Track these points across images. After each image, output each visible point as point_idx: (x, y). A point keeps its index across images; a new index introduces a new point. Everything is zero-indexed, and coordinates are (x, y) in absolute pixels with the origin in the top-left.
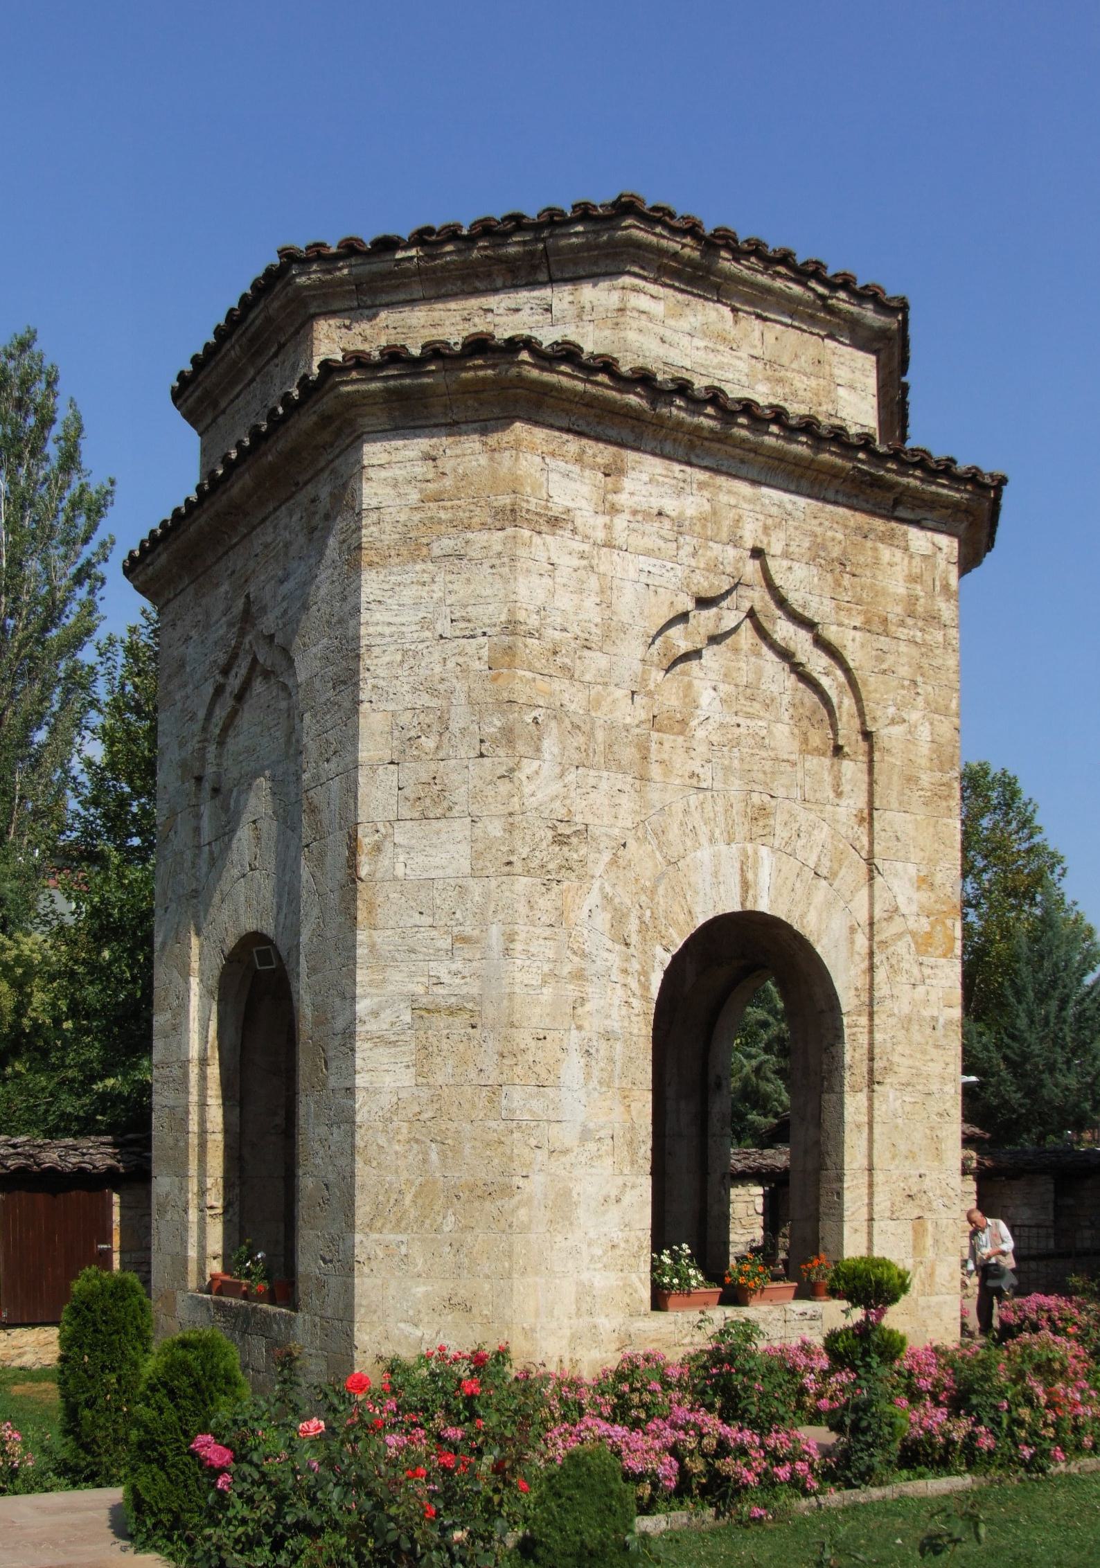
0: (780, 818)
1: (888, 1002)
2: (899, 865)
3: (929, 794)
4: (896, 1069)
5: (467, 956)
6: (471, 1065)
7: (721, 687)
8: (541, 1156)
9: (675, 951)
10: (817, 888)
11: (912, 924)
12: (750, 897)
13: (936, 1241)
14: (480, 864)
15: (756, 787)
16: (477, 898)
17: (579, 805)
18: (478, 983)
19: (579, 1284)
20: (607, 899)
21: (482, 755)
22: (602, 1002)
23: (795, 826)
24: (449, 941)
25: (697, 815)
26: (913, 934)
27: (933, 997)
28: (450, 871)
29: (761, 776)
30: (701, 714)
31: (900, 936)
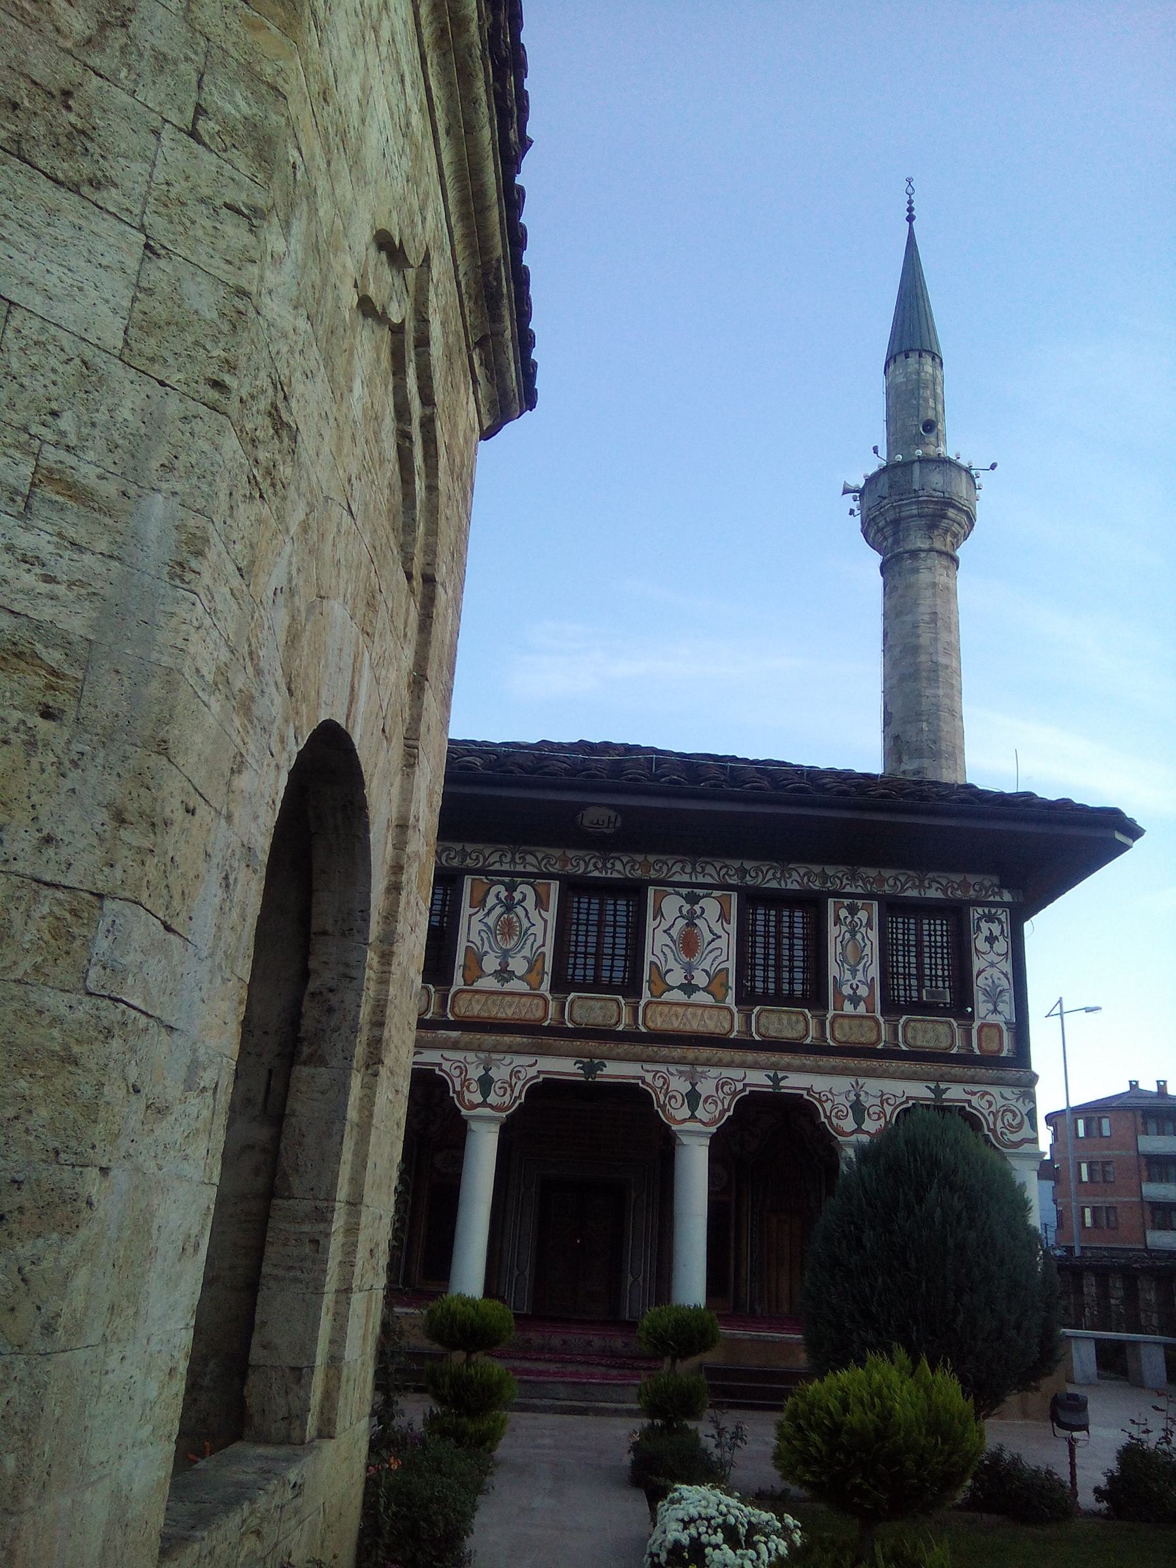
5: (71, 533)
6: (22, 817)
14: (150, 346)
16: (127, 414)
18: (88, 611)
21: (194, 134)
24: (27, 470)
28: (63, 312)
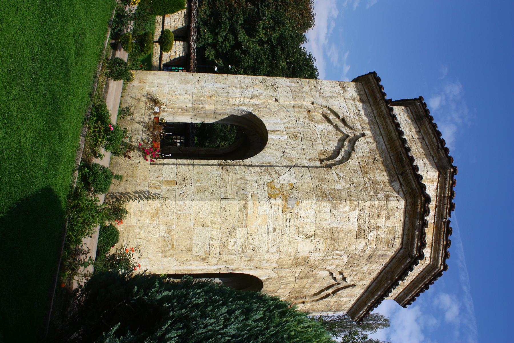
0: (296, 142)
1: (249, 172)
2: (294, 176)
3: (321, 188)
4: (228, 174)
7: (325, 131)
8: (198, 78)
9: (252, 112)
10: (280, 152)
11: (276, 181)
12: (272, 132)
13: (168, 190)
15: (302, 135)
17: (282, 89)
19: (165, 85)
20: (262, 94)
22: (236, 92)
23: (295, 146)
25: (289, 119)
26: (273, 181)
27: (254, 189)
29: (306, 137)
30: (316, 125)
31: (271, 176)
